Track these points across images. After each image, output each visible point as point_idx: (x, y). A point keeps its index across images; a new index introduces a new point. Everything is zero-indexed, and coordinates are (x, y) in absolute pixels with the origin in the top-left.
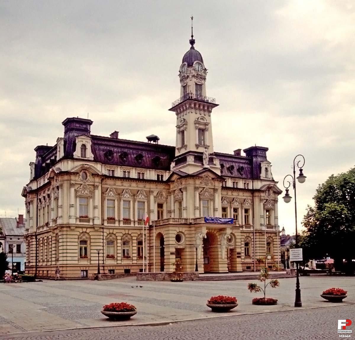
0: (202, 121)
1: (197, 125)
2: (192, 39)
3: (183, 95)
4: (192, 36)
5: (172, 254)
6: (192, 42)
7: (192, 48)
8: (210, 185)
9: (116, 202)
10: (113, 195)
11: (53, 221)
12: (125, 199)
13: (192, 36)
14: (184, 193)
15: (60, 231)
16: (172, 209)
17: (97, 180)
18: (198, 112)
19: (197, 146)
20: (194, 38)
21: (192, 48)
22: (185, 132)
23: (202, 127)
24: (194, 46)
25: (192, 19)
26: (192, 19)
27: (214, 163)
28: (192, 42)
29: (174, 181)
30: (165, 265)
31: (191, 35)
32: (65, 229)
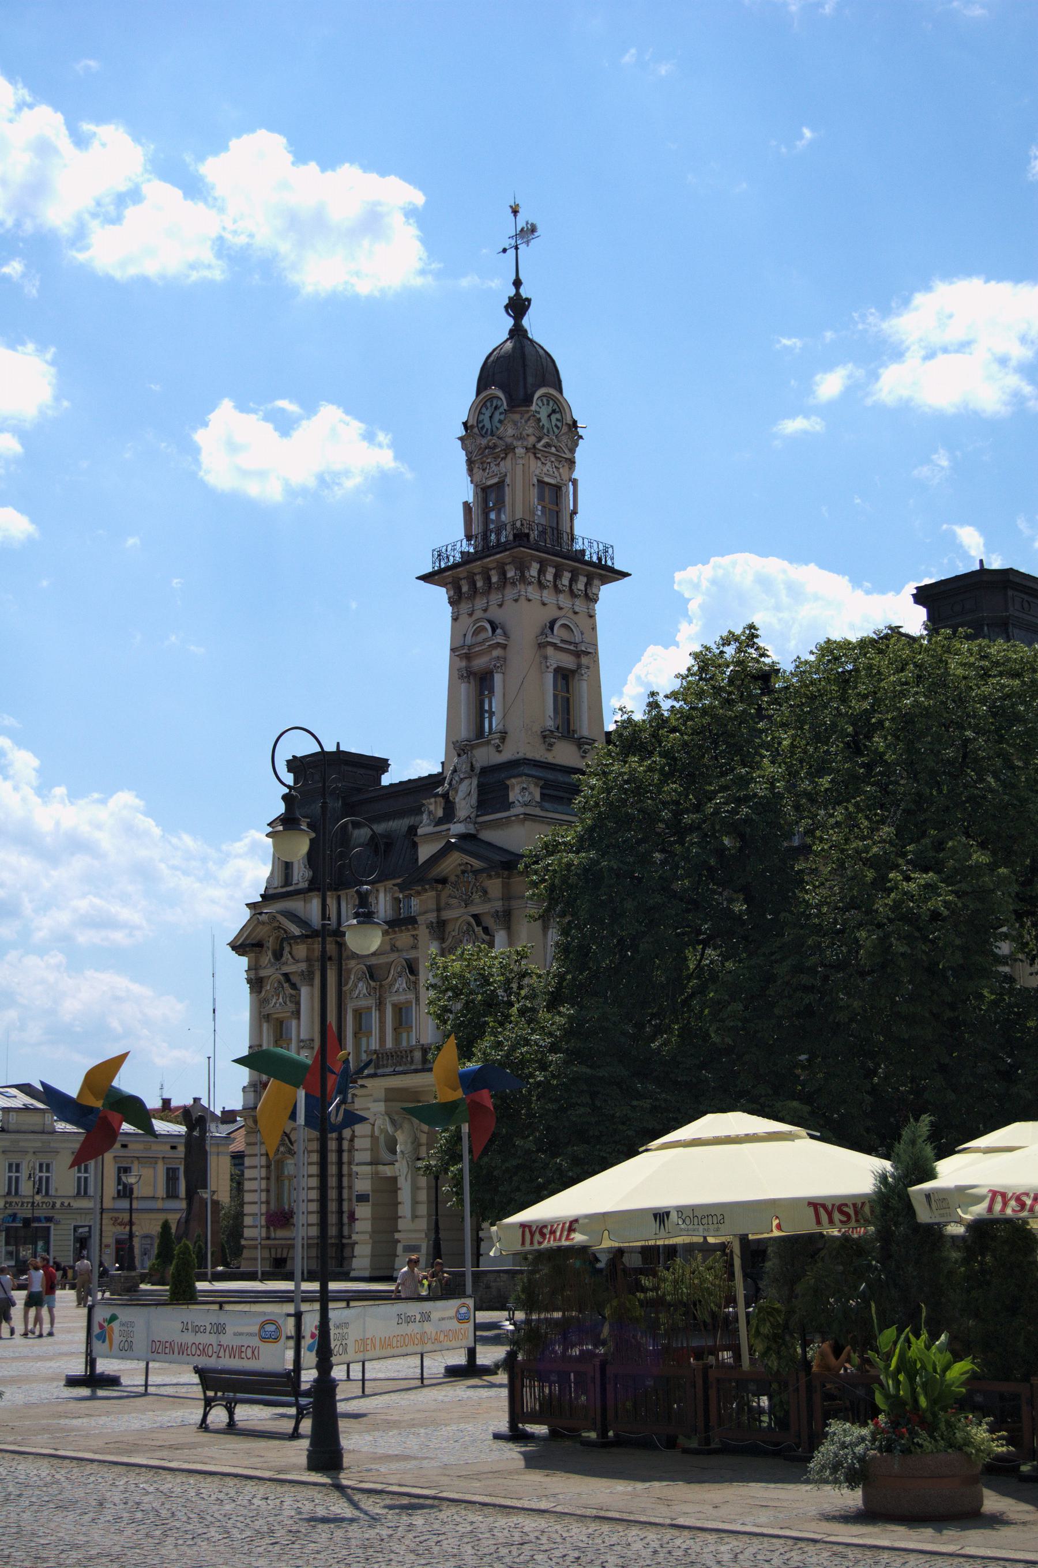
0: (483, 636)
1: (464, 664)
2: (518, 294)
4: (517, 283)
5: (362, 1198)
6: (518, 306)
7: (518, 333)
8: (476, 897)
9: (375, 1015)
10: (365, 991)
12: (395, 999)
13: (517, 283)
17: (301, 950)
18: (480, 603)
19: (547, 737)
23: (480, 663)
25: (515, 212)
26: (515, 212)
27: (511, 799)
28: (518, 306)
30: (244, 1247)
31: (514, 277)
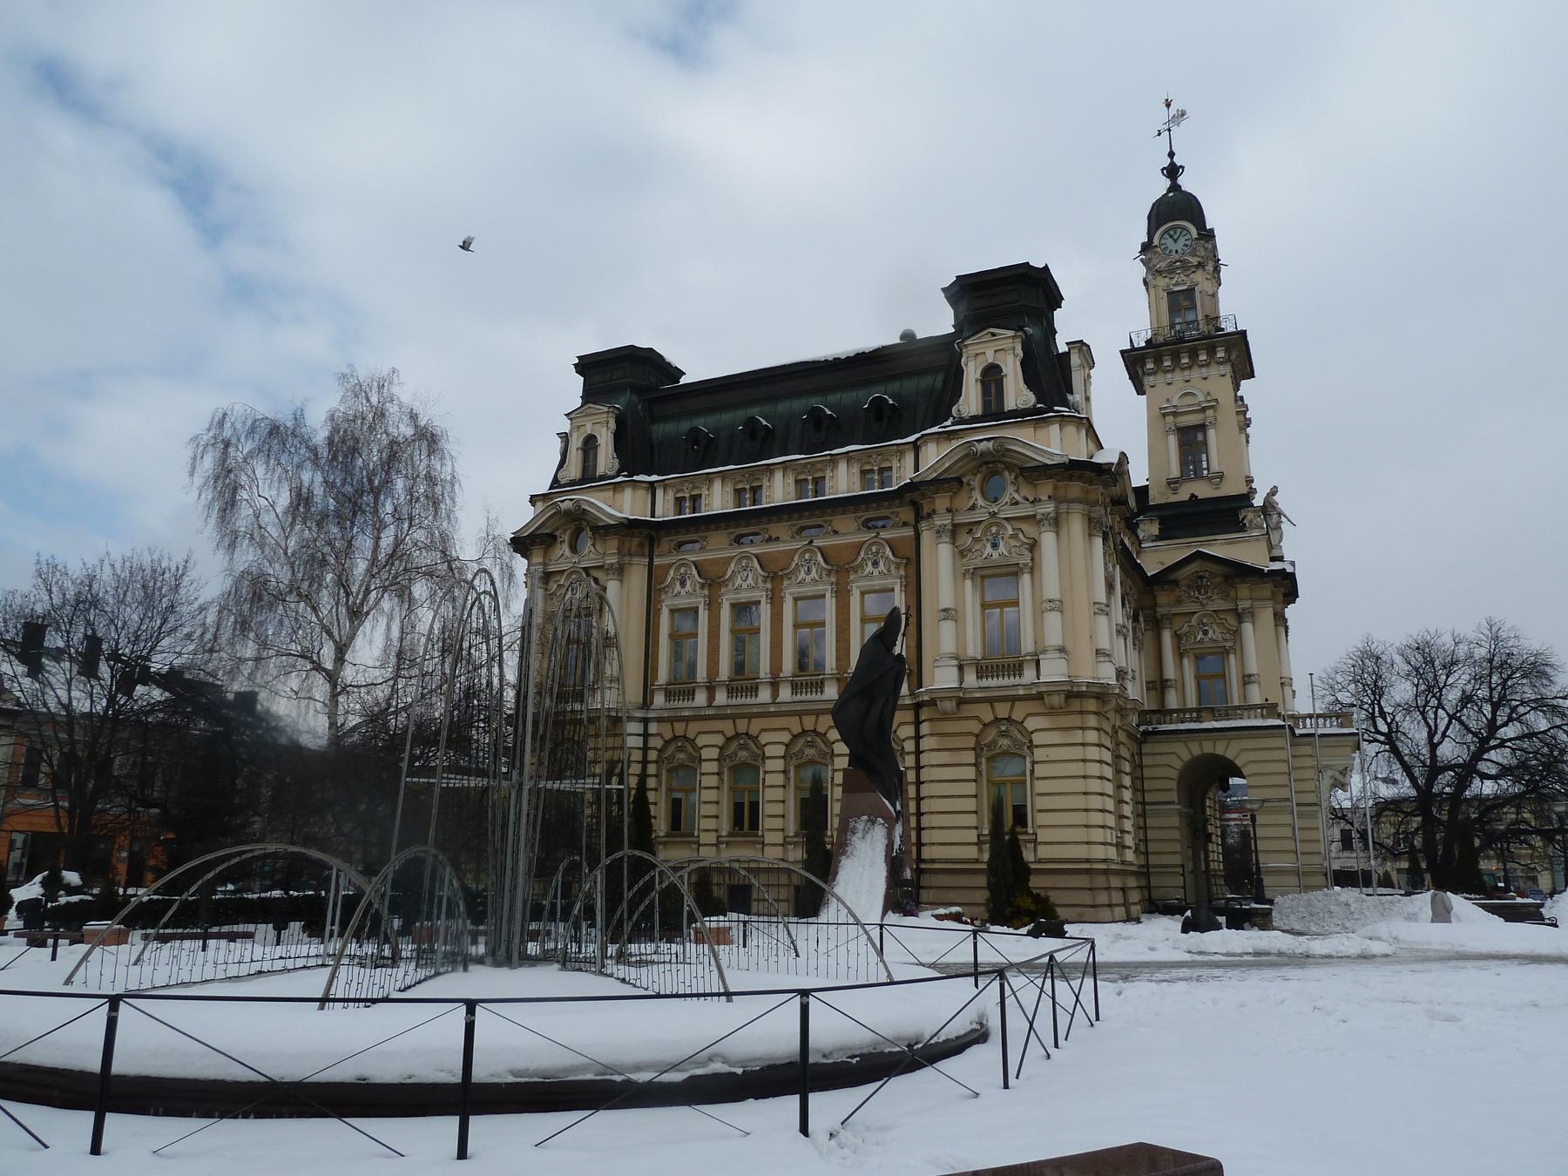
3: (1165, 321)
4: (1171, 154)
6: (1173, 171)
7: (1175, 187)
11: (961, 668)
13: (1171, 154)
14: (1247, 628)
15: (1052, 711)
16: (1170, 672)
20: (1178, 161)
21: (1175, 187)
22: (1211, 433)
24: (1180, 181)
25: (1168, 105)
26: (1168, 105)
28: (1173, 171)
29: (1176, 583)
32: (1092, 705)
